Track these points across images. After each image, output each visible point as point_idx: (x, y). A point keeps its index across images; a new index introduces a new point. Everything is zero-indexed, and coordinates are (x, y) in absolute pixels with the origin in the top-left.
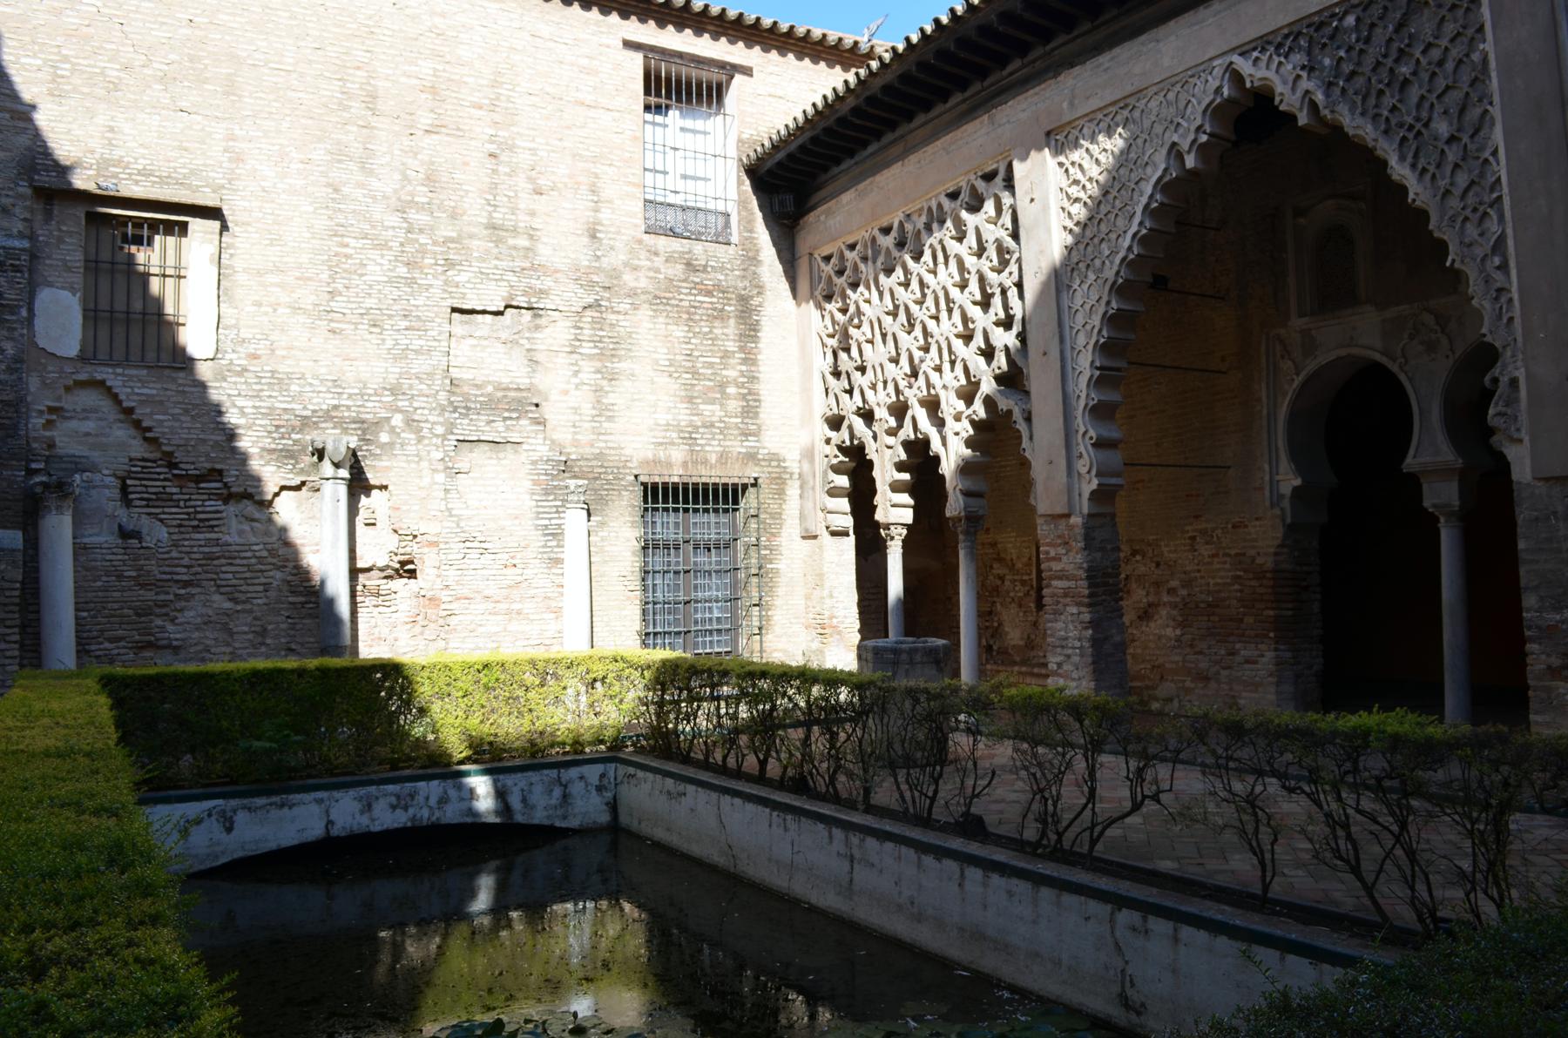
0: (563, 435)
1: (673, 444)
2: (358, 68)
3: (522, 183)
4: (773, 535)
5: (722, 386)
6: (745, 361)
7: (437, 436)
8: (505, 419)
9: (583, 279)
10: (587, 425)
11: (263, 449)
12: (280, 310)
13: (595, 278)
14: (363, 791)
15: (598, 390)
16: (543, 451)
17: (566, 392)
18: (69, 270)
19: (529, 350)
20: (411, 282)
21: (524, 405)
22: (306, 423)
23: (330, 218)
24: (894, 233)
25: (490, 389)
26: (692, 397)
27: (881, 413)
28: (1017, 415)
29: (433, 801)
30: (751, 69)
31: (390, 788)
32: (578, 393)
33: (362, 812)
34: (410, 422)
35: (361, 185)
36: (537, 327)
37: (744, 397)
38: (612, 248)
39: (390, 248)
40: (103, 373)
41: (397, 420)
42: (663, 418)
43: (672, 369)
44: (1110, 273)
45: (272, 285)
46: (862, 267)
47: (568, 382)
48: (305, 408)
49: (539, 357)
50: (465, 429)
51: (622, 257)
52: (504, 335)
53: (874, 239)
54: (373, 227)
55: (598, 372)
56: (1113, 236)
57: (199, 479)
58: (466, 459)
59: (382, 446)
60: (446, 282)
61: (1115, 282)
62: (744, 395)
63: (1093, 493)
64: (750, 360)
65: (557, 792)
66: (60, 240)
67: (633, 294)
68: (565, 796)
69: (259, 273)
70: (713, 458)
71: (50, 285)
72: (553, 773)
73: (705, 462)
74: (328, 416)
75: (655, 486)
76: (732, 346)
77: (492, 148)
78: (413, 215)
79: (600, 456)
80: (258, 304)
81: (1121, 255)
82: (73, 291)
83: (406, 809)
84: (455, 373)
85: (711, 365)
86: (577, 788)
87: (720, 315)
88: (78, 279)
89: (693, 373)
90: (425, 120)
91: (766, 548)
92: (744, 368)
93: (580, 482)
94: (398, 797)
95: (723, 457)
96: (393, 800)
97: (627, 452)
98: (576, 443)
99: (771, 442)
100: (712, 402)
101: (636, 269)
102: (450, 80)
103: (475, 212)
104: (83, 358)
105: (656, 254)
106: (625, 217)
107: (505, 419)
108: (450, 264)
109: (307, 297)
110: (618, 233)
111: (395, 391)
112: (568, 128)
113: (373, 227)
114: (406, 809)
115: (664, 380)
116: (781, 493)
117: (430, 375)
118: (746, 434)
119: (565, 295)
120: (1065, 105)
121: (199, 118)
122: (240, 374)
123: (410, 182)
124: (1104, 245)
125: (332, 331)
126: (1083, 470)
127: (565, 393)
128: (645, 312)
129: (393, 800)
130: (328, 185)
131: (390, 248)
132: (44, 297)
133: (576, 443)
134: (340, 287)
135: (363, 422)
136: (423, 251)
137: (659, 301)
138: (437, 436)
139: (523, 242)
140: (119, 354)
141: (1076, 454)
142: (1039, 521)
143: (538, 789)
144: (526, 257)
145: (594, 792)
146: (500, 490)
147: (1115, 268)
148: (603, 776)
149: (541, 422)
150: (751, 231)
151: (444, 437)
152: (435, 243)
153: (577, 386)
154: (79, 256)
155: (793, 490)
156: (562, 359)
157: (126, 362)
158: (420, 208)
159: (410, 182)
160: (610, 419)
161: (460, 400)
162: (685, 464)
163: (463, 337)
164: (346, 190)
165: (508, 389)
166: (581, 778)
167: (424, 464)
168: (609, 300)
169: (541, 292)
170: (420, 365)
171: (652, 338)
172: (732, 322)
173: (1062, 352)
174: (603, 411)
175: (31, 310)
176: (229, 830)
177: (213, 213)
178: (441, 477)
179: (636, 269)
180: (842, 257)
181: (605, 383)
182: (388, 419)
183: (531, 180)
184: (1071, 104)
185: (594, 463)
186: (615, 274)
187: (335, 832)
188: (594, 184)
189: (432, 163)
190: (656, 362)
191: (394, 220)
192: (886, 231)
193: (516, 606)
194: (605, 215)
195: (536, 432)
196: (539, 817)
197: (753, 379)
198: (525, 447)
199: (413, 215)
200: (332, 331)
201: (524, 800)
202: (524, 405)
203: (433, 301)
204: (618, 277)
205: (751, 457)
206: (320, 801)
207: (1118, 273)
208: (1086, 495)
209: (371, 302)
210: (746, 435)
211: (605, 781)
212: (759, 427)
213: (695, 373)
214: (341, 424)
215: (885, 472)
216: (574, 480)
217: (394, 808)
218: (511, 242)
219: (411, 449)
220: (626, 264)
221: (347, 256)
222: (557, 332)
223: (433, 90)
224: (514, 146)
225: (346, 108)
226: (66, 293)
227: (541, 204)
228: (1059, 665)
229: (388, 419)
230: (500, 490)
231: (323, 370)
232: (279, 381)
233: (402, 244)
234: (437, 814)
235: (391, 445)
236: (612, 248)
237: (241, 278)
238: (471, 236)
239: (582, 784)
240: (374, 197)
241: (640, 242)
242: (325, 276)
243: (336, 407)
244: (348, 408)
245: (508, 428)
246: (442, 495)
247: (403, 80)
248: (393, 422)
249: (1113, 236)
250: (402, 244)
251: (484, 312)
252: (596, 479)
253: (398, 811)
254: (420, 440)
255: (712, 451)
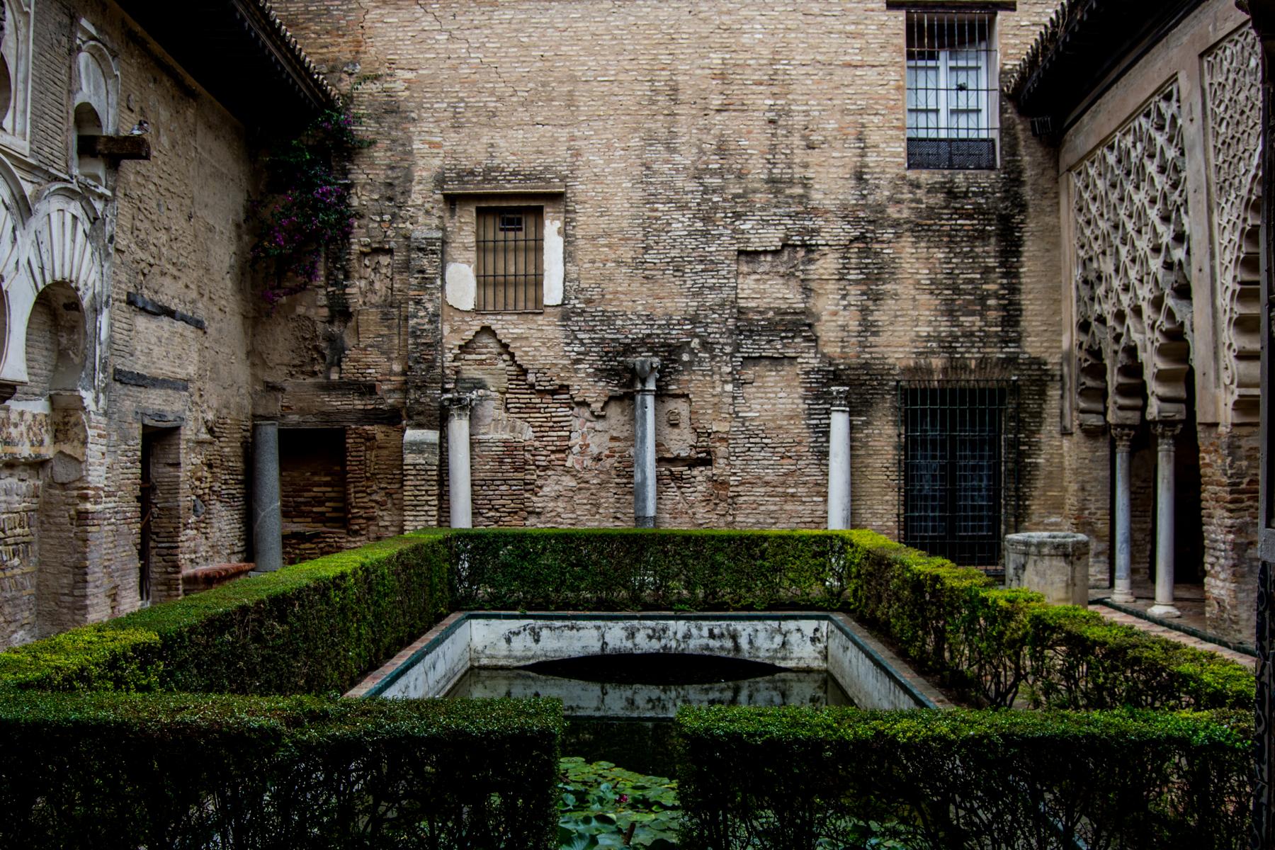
0: (833, 350)
1: (933, 353)
2: (663, 69)
3: (796, 140)
4: (1033, 432)
5: (983, 299)
6: (1005, 275)
7: (726, 354)
8: (782, 338)
9: (848, 215)
10: (854, 340)
11: (596, 369)
12: (609, 264)
13: (862, 215)
14: (629, 623)
15: (864, 311)
16: (815, 363)
17: (835, 314)
18: (466, 249)
19: (803, 280)
20: (705, 234)
21: (798, 325)
22: (628, 349)
23: (644, 190)
24: (1115, 152)
25: (771, 314)
26: (953, 311)
27: (1111, 322)
28: (1187, 328)
29: (679, 636)
30: (1014, 4)
31: (649, 623)
32: (846, 313)
33: (627, 638)
34: (705, 345)
35: (667, 162)
36: (811, 261)
37: (1004, 308)
38: (877, 187)
39: (690, 209)
40: (489, 321)
41: (695, 343)
42: (924, 330)
43: (935, 287)
44: (1244, 192)
45: (603, 246)
46: (1098, 182)
47: (837, 305)
48: (627, 337)
49: (813, 285)
50: (748, 347)
51: (887, 193)
52: (782, 270)
53: (1104, 158)
54: (677, 193)
55: (863, 294)
56: (1247, 155)
57: (553, 393)
58: (749, 374)
59: (684, 364)
60: (734, 231)
61: (1249, 199)
62: (1005, 306)
63: (1235, 403)
64: (1011, 273)
65: (778, 639)
66: (461, 229)
67: (896, 224)
68: (784, 644)
69: (593, 239)
70: (973, 364)
71: (455, 261)
72: (775, 624)
73: (965, 368)
74: (643, 341)
75: (914, 391)
76: (991, 262)
77: (771, 115)
78: (707, 180)
79: (866, 365)
80: (593, 262)
81: (1253, 172)
82: (468, 262)
83: (659, 639)
84: (742, 303)
85: (971, 281)
86: (794, 638)
87: (982, 236)
88: (472, 255)
89: (954, 290)
90: (716, 102)
91: (1024, 444)
92: (1005, 281)
93: (842, 389)
94: (654, 630)
95: (983, 362)
96: (650, 632)
97: (890, 361)
98: (844, 356)
99: (1033, 346)
100: (973, 313)
101: (899, 202)
102: (735, 65)
103: (757, 170)
104: (478, 311)
105: (918, 187)
106: (889, 155)
107: (782, 338)
108: (737, 216)
109: (627, 254)
110: (883, 172)
111: (694, 320)
112: (837, 88)
113: (677, 193)
114: (659, 639)
115: (924, 298)
116: (1042, 394)
117: (722, 305)
118: (1006, 341)
119: (834, 231)
120: (1210, 28)
121: (550, 128)
122: (579, 315)
123: (705, 153)
124: (1242, 164)
125: (646, 278)
126: (1228, 382)
127: (834, 314)
128: (908, 239)
129: (650, 632)
130: (643, 165)
131: (690, 209)
132: (451, 269)
133: (844, 356)
134: (651, 243)
135: (670, 345)
136: (715, 207)
137: (920, 228)
138: (726, 354)
139: (798, 190)
140: (500, 307)
141: (1222, 365)
142: (1199, 428)
143: (762, 635)
144: (801, 203)
145: (809, 642)
146: (776, 398)
147: (1248, 186)
148: (816, 630)
149: (814, 340)
150: (1014, 155)
151: (732, 355)
152: (725, 200)
153: (845, 307)
154: (473, 239)
155: (1053, 393)
156: (831, 286)
157: (505, 312)
158: (713, 173)
159: (705, 153)
160: (875, 334)
161: (745, 325)
162: (945, 371)
163: (749, 274)
164: (655, 167)
165: (786, 313)
166: (799, 630)
167: (716, 377)
168: (873, 232)
169: (813, 230)
170: (712, 298)
171: (914, 262)
172: (993, 240)
173: (1212, 268)
174: (868, 328)
175: (443, 280)
176: (537, 641)
177: (557, 198)
178: (729, 387)
179: (899, 202)
180: (1087, 174)
181: (870, 303)
182: (689, 343)
183: (804, 137)
184: (1215, 29)
185: (860, 372)
186: (880, 208)
187: (608, 651)
188: (861, 133)
189: (723, 135)
190: (918, 282)
191: (691, 185)
192: (1111, 148)
193: (791, 490)
194: (871, 159)
195: (809, 348)
196: (763, 656)
197: (1014, 290)
198: (799, 360)
199: (707, 180)
200: (646, 278)
201: (751, 642)
202: (798, 325)
203: (722, 246)
204: (882, 212)
205: (1011, 361)
206: (598, 628)
207: (1250, 191)
208: (1230, 405)
209: (674, 253)
210: (1006, 342)
211: (818, 635)
212: (1020, 334)
213: (956, 290)
214: (653, 350)
215: (1113, 379)
216: (850, 386)
217: (650, 637)
218: (788, 191)
219: (706, 366)
220: (890, 199)
221: (657, 219)
222: (827, 264)
223: (722, 76)
224: (790, 111)
225: (654, 103)
226: (465, 266)
227: (814, 157)
228: (1212, 565)
229: (689, 343)
230: (776, 398)
231: (640, 308)
232: (608, 319)
233: (699, 204)
234: (683, 646)
235: (691, 363)
236: (877, 187)
237: (581, 243)
238: (754, 191)
239: (799, 635)
240: (677, 170)
241: (903, 178)
242: (640, 236)
243: (649, 336)
244: (658, 335)
245: (785, 346)
246: (730, 400)
247: (699, 72)
248: (693, 345)
249: (1247, 155)
250: (699, 204)
251: (765, 252)
252: (862, 385)
253: (654, 641)
254: (713, 358)
255: (972, 357)
